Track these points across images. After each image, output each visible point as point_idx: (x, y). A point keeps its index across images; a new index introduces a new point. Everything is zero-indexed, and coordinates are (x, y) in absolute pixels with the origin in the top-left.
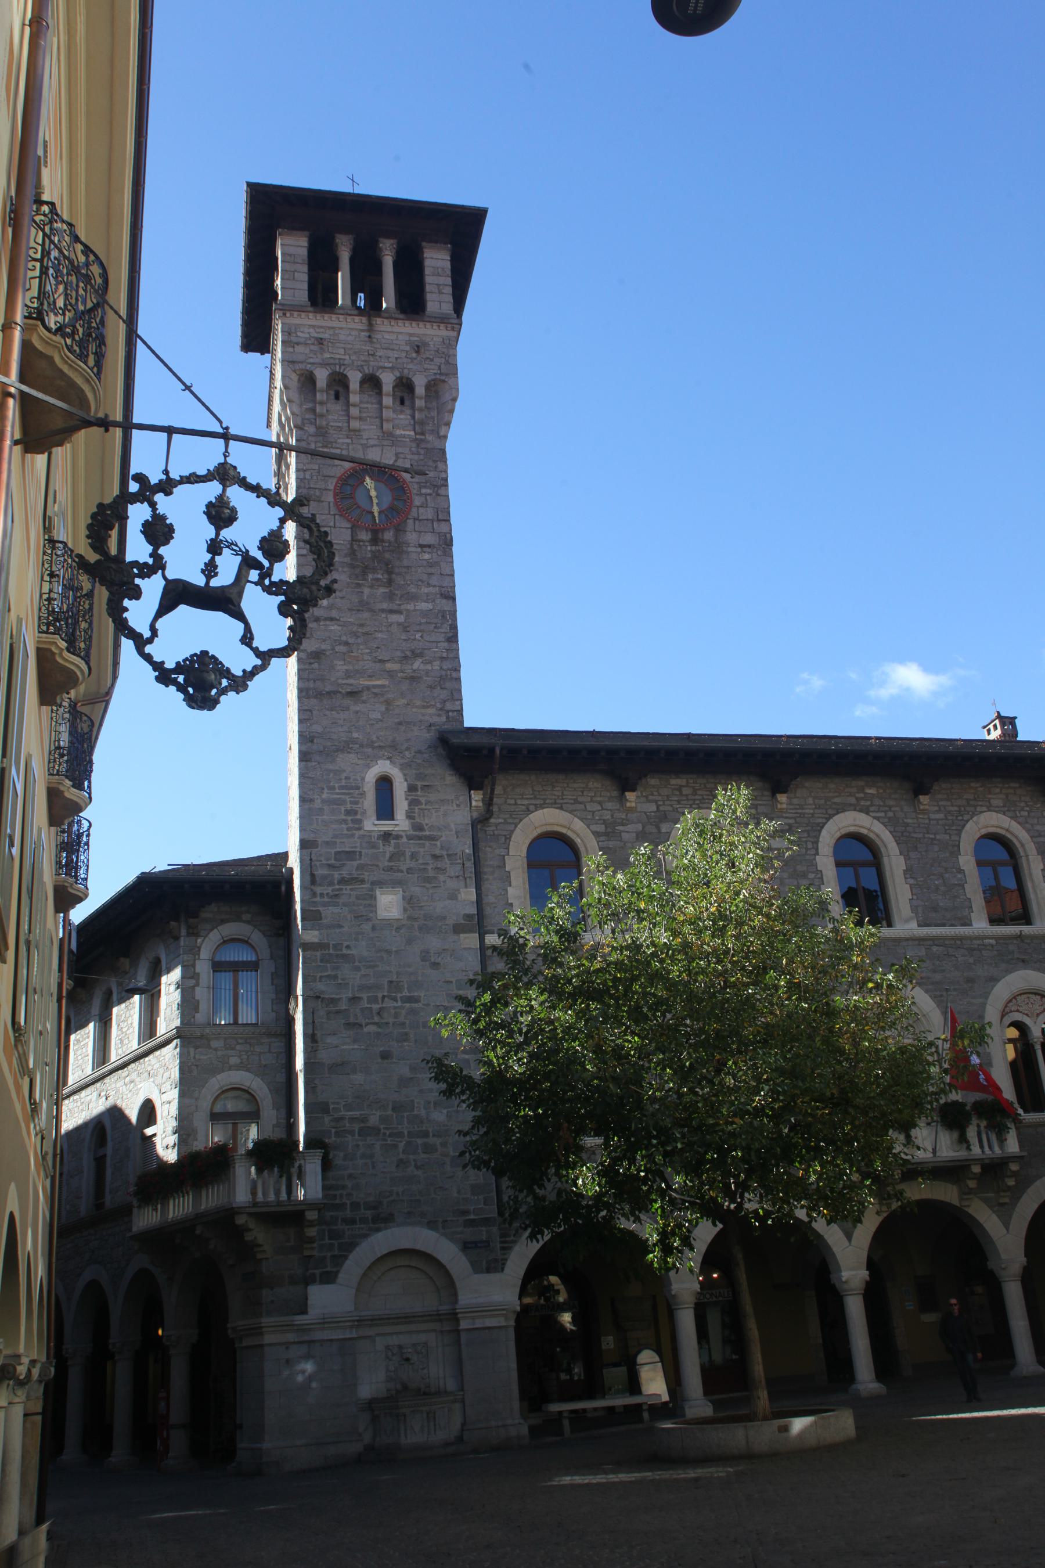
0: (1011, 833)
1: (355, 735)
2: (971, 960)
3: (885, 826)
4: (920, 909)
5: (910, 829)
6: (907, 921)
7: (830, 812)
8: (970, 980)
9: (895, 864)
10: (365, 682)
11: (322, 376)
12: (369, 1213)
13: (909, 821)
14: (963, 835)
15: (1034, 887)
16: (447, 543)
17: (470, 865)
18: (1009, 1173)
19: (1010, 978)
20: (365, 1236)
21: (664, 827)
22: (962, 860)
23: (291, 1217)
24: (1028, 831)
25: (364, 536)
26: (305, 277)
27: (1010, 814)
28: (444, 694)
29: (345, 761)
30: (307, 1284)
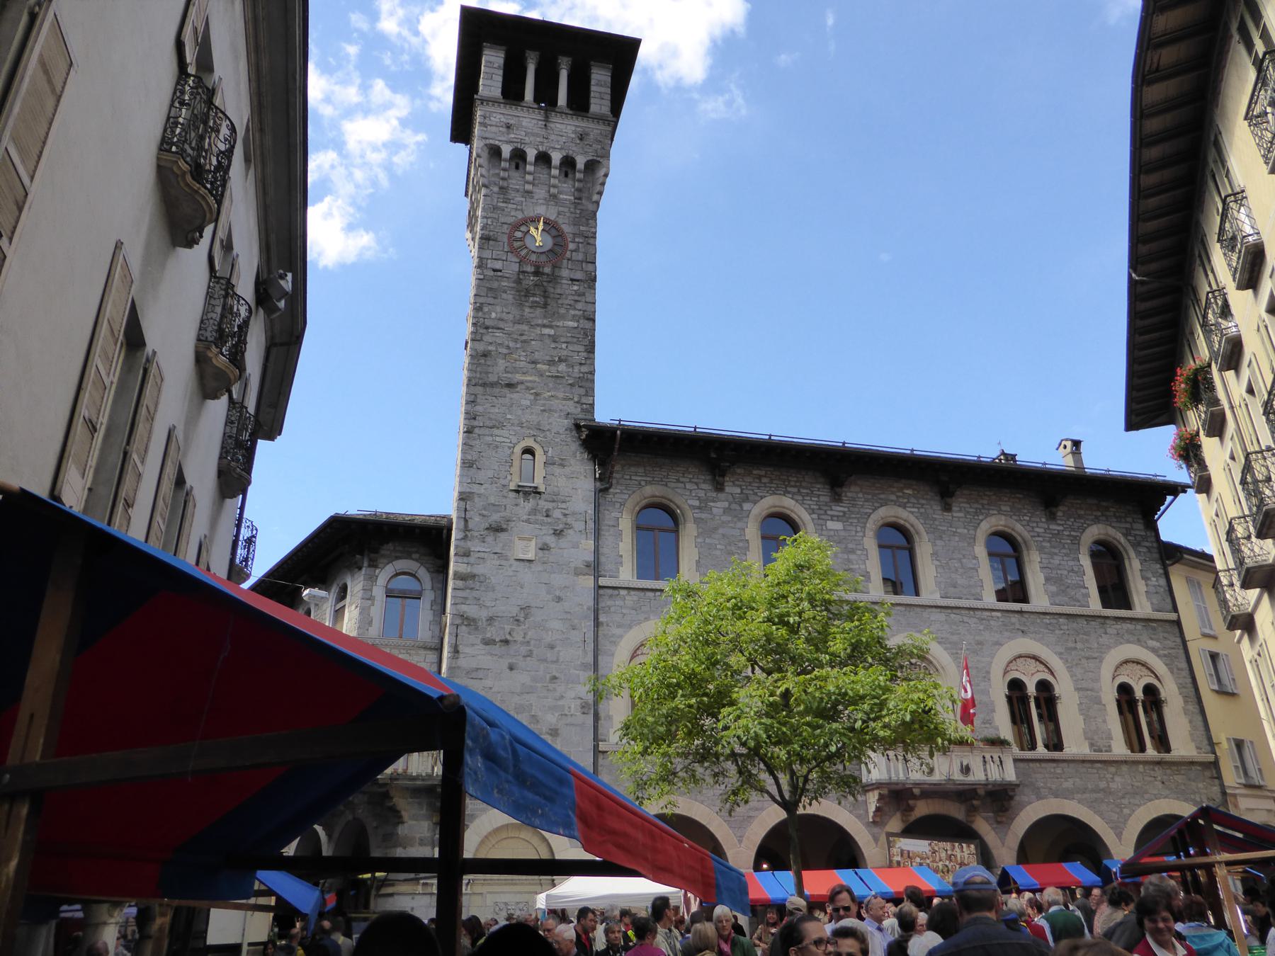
8: (980, 643)
9: (924, 550)
10: (519, 377)
11: (506, 150)
16: (591, 280)
17: (591, 525)
19: (1012, 643)
21: (746, 506)
25: (530, 269)
26: (500, 79)
28: (582, 391)
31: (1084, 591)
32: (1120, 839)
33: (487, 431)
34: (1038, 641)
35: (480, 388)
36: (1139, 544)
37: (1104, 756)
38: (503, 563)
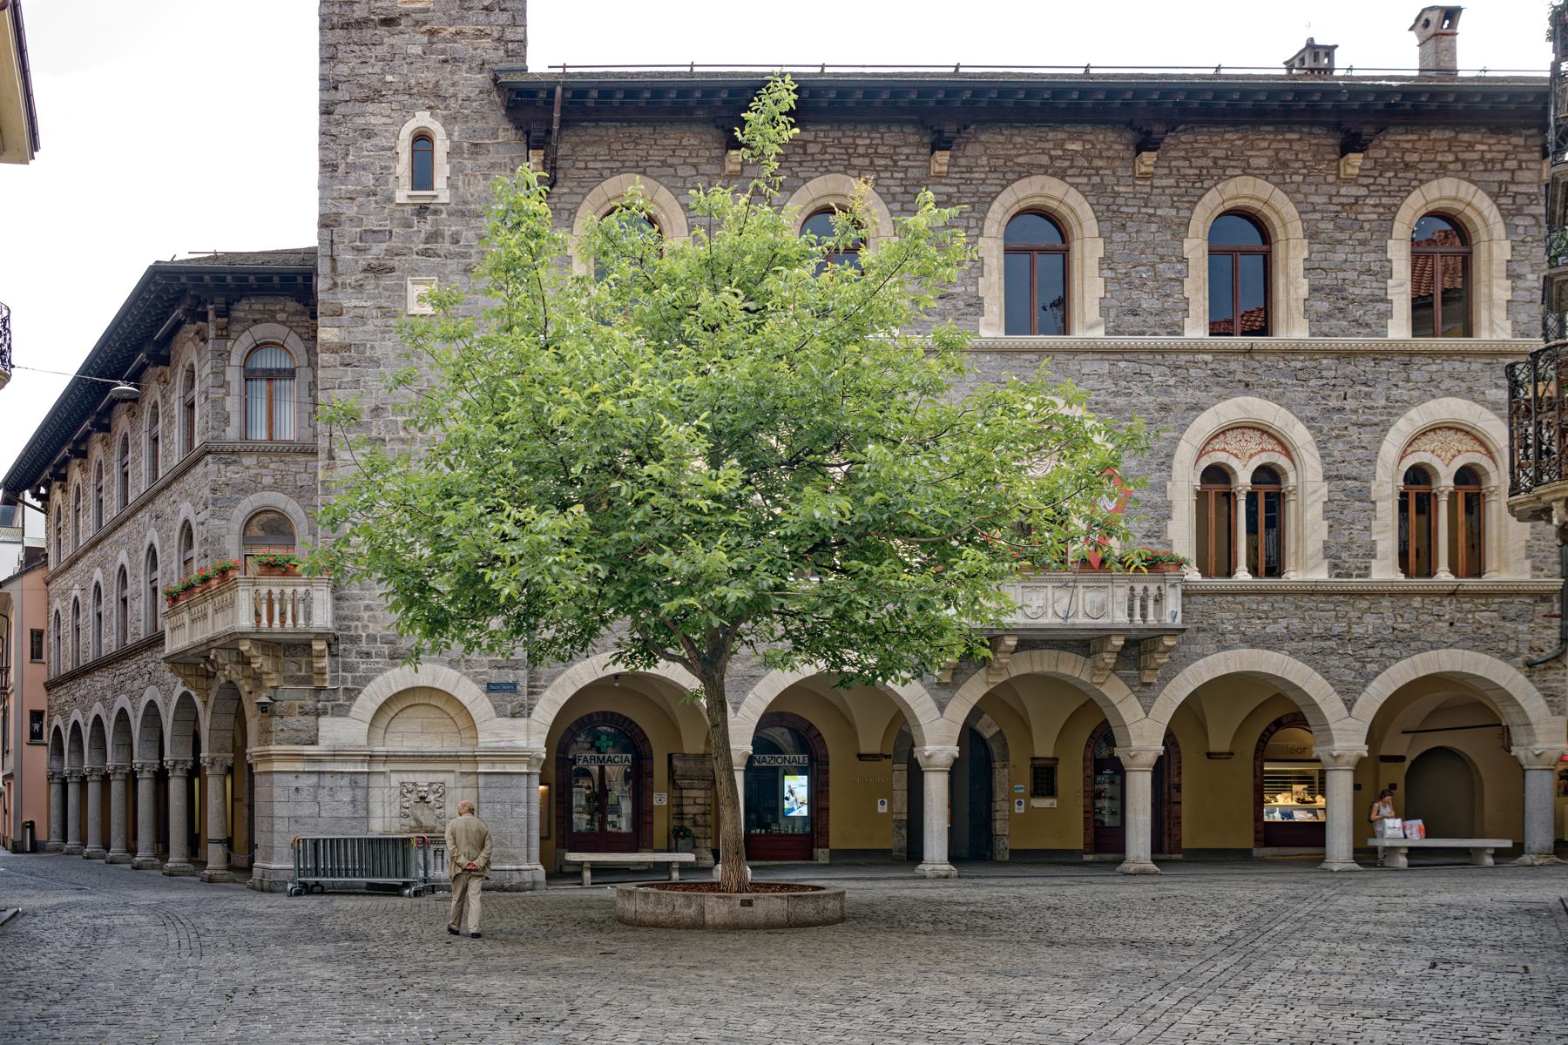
0: (1272, 208)
1: (389, 78)
2: (1171, 382)
3: (1086, 197)
4: (1112, 314)
5: (1120, 201)
6: (1091, 327)
7: (1010, 176)
9: (1088, 250)
12: (386, 649)
13: (1122, 189)
14: (1198, 209)
15: (1287, 285)
18: (1161, 649)
20: (381, 671)
22: (1187, 244)
23: (294, 648)
24: (1297, 203)
27: (1276, 179)
28: (504, 18)
29: (375, 116)
30: (318, 715)
31: (1382, 307)
32: (1350, 709)
33: (358, 107)
34: (1276, 399)
35: (339, 32)
36: (1519, 212)
37: (1354, 583)
38: (392, 322)
